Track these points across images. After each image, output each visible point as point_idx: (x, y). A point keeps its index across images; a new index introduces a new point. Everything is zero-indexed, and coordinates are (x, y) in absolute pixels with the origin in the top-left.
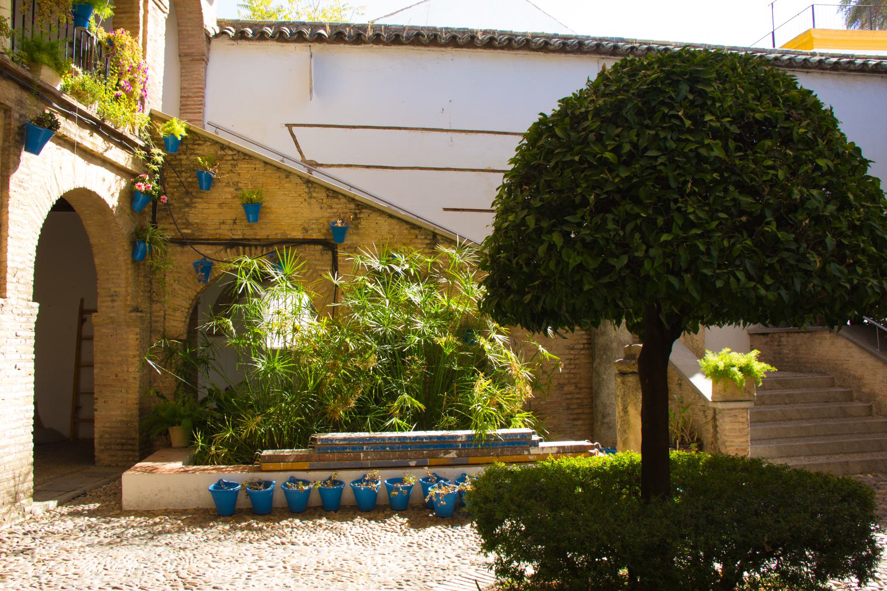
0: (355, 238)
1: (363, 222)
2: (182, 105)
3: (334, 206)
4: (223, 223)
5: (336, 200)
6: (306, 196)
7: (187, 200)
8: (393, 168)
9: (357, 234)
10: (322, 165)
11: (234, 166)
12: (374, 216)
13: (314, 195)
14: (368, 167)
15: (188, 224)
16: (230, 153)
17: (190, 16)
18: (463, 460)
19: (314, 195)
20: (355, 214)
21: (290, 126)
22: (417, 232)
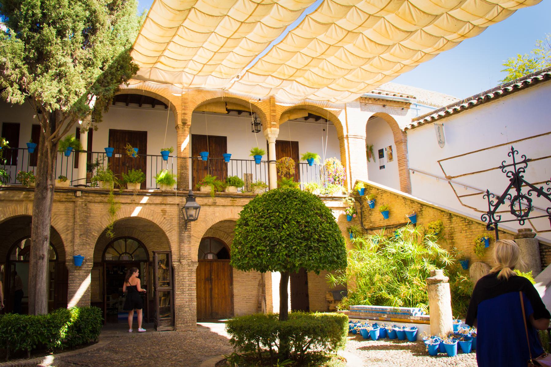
0: (422, 219)
1: (424, 212)
2: (399, 164)
3: (414, 207)
4: (381, 220)
5: (414, 204)
6: (404, 204)
7: (370, 212)
8: (484, 171)
9: (422, 218)
10: (454, 177)
11: (382, 196)
12: (427, 208)
13: (407, 203)
14: (473, 173)
15: (371, 222)
16: (380, 191)
17: (394, 125)
18: (389, 319)
19: (407, 203)
20: (421, 209)
21: (439, 162)
22: (443, 213)
